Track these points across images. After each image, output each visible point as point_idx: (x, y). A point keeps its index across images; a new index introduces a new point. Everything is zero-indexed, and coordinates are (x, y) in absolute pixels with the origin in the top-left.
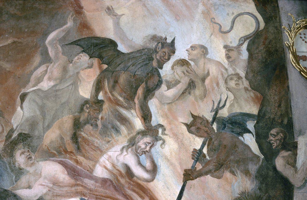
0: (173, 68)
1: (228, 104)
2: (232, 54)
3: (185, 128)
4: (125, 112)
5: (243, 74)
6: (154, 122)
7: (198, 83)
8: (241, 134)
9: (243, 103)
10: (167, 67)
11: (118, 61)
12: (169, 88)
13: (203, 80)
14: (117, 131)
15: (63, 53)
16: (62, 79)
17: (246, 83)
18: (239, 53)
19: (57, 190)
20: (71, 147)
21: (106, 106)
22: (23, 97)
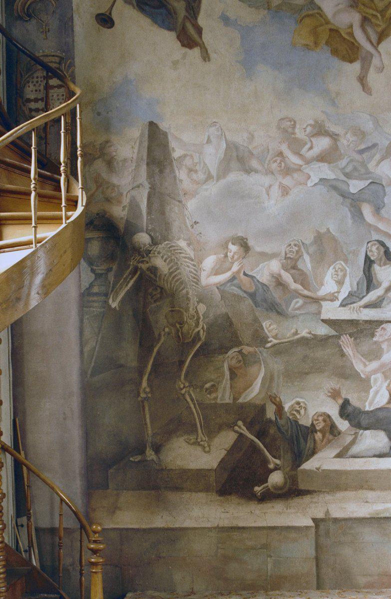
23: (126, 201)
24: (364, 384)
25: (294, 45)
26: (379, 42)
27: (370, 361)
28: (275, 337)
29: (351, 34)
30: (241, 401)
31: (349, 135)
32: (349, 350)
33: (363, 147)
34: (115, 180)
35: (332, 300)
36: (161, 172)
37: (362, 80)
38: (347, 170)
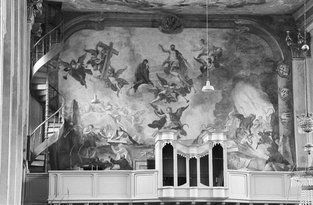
0: (255, 121)
2: (268, 118)
4: (245, 131)
5: (270, 123)
6: (252, 133)
7: (260, 125)
8: (269, 136)
10: (254, 121)
12: (254, 126)
13: (261, 124)
16: (233, 123)
17: (270, 125)
20: (235, 138)
21: (242, 129)
22: (225, 127)
23: (68, 116)
24: (116, 155)
26: (121, 88)
28: (98, 145)
29: (116, 86)
30: (90, 158)
31: (114, 106)
32: (113, 148)
33: (117, 108)
36: (76, 110)
37: (117, 95)
38: (114, 113)
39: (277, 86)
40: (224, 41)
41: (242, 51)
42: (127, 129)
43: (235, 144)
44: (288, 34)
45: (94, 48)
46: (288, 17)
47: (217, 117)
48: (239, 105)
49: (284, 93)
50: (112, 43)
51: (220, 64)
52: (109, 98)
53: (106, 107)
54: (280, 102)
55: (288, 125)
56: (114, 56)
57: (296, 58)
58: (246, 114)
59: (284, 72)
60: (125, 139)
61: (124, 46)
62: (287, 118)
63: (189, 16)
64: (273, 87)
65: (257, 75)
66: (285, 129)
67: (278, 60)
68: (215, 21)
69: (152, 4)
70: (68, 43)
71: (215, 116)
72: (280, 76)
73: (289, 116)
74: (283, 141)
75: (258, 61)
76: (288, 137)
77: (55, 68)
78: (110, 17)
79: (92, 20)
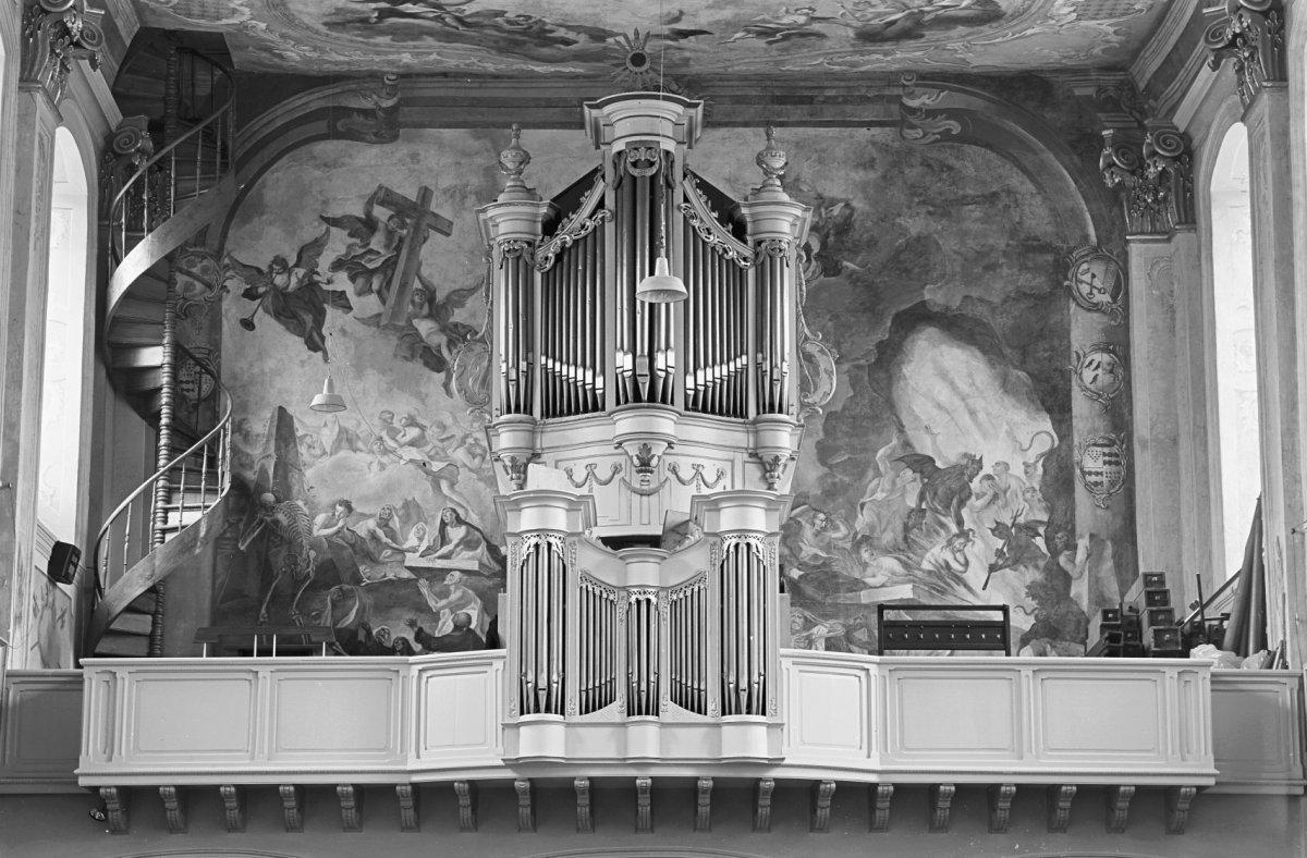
1: (1024, 513)
2: (1030, 470)
3: (990, 532)
4: (943, 519)
5: (1037, 488)
6: (966, 528)
8: (1033, 537)
9: (1036, 512)
10: (976, 480)
11: (936, 476)
12: (977, 499)
13: (1005, 492)
14: (938, 533)
15: (892, 469)
16: (892, 491)
17: (1040, 496)
18: (1035, 469)
19: (895, 578)
21: (928, 514)
22: (862, 506)
23: (257, 468)
24: (435, 617)
25: (395, 356)
27: (441, 599)
29: (439, 351)
32: (424, 591)
33: (444, 436)
34: (249, 451)
35: (414, 552)
37: (446, 386)
38: (432, 453)
39: (1069, 347)
40: (859, 176)
41: (929, 213)
42: (482, 519)
43: (898, 568)
44: (1108, 142)
45: (358, 211)
46: (1110, 79)
47: (830, 467)
48: (917, 418)
49: (1096, 372)
50: (426, 189)
51: (845, 263)
52: (414, 401)
53: (401, 434)
54: (1080, 405)
55: (1111, 494)
56: (436, 238)
57: (1142, 233)
58: (946, 453)
59: (1095, 291)
60: (471, 553)
61: (472, 199)
62: (1106, 468)
63: (726, 83)
64: (1052, 349)
65: (990, 303)
66: (1099, 512)
67: (1072, 244)
68: (829, 97)
69: (561, 33)
70: (260, 196)
71: (823, 460)
72: (1078, 305)
73: (1113, 459)
74: (1089, 556)
75: (992, 249)
76: (1109, 543)
77: (209, 286)
78: (417, 93)
79: (354, 103)
